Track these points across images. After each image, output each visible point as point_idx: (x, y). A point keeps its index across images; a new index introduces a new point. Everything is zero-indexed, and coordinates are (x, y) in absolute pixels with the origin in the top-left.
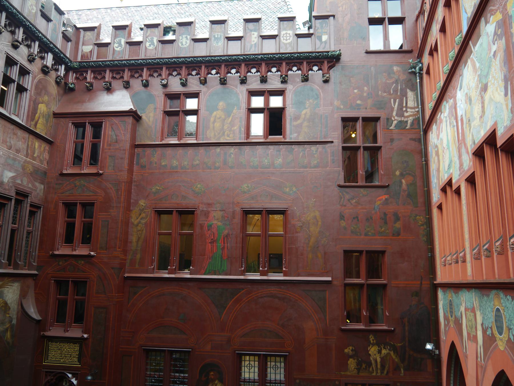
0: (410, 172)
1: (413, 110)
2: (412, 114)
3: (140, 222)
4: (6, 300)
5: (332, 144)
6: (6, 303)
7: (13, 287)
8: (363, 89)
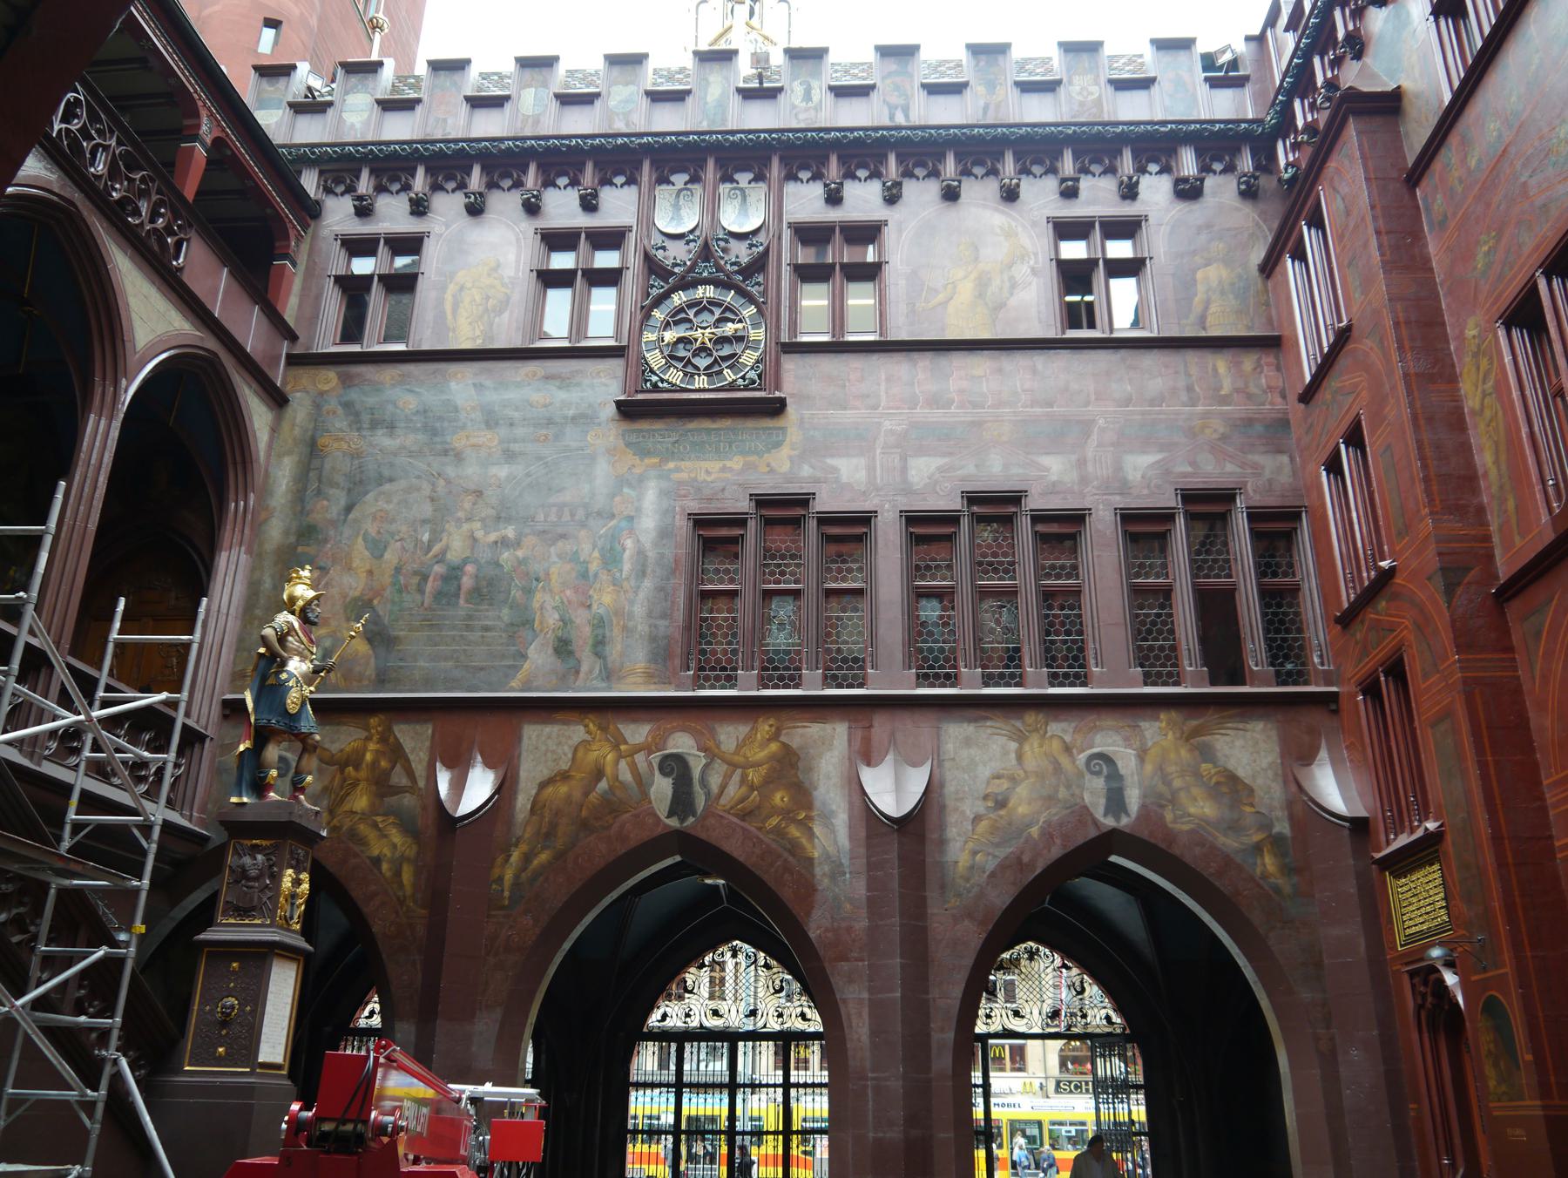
3: (1484, 395)
4: (1230, 767)
6: (1232, 778)
7: (1249, 734)
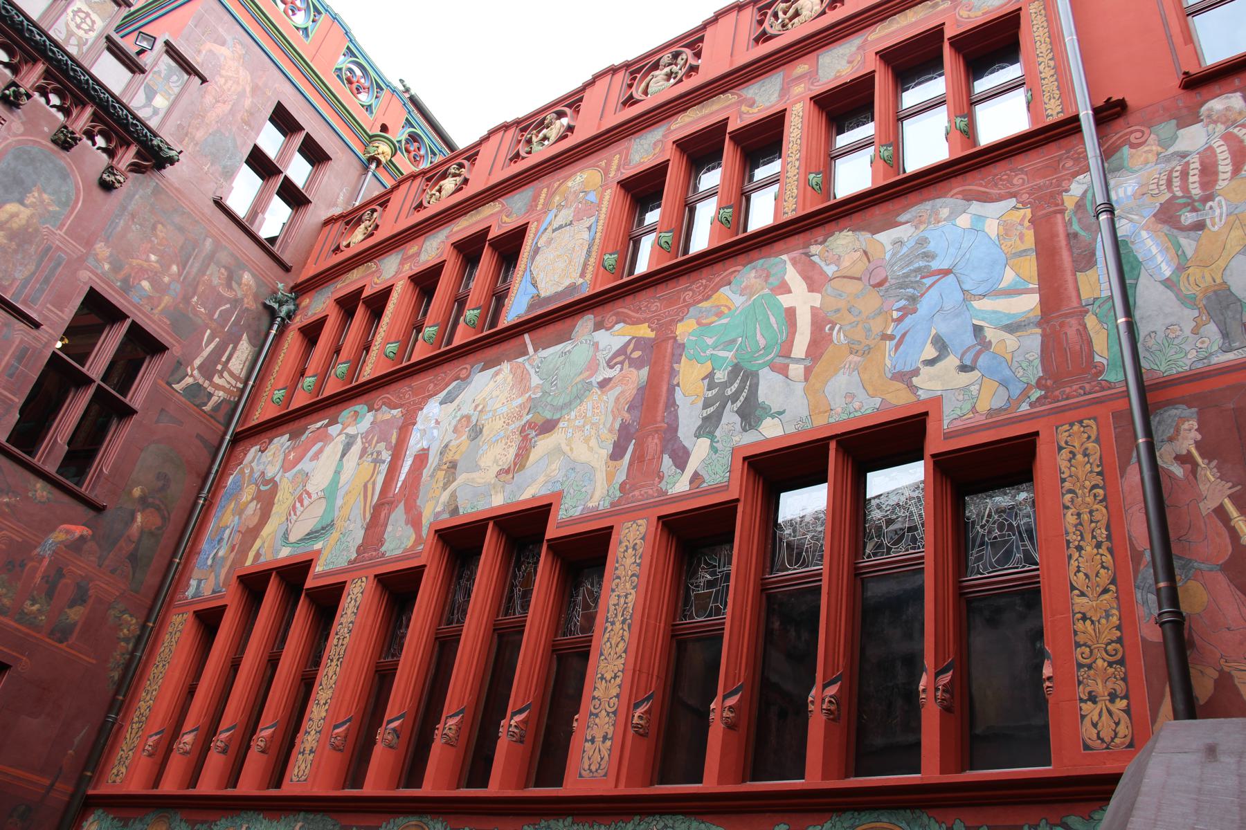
0: (162, 507)
1: (233, 382)
2: (228, 386)
5: (35, 332)
8: (169, 267)
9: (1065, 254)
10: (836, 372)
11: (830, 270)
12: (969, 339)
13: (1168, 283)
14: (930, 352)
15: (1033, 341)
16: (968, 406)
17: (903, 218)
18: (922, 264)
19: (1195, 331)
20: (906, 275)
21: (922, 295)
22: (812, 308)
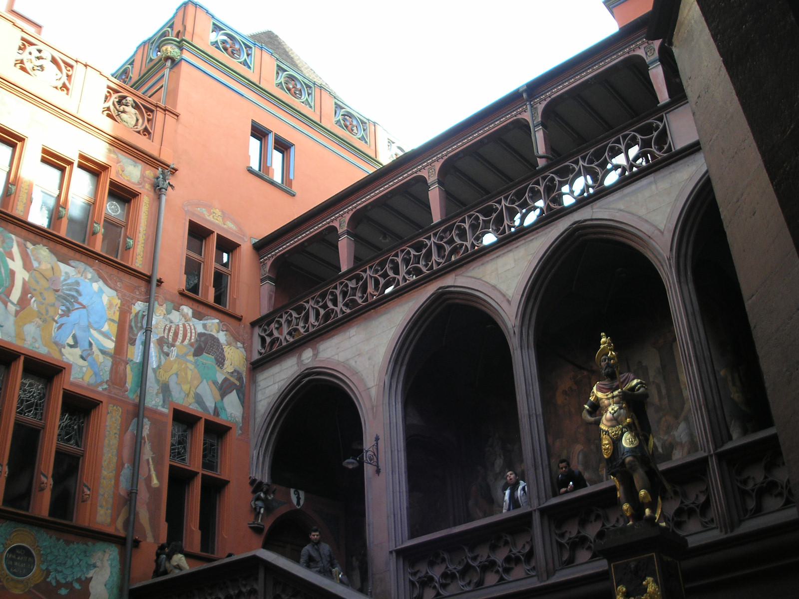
9: (127, 333)
10: (31, 322)
11: (35, 264)
12: (87, 346)
13: (154, 370)
14: (72, 343)
15: (109, 362)
16: (81, 376)
17: (71, 262)
18: (74, 293)
19: (157, 394)
20: (69, 295)
21: (73, 310)
22: (24, 279)
